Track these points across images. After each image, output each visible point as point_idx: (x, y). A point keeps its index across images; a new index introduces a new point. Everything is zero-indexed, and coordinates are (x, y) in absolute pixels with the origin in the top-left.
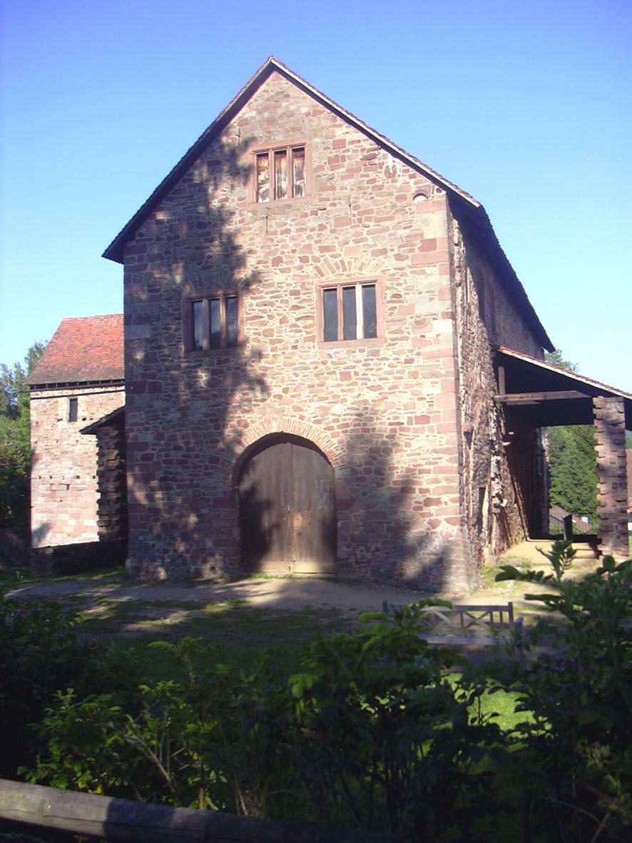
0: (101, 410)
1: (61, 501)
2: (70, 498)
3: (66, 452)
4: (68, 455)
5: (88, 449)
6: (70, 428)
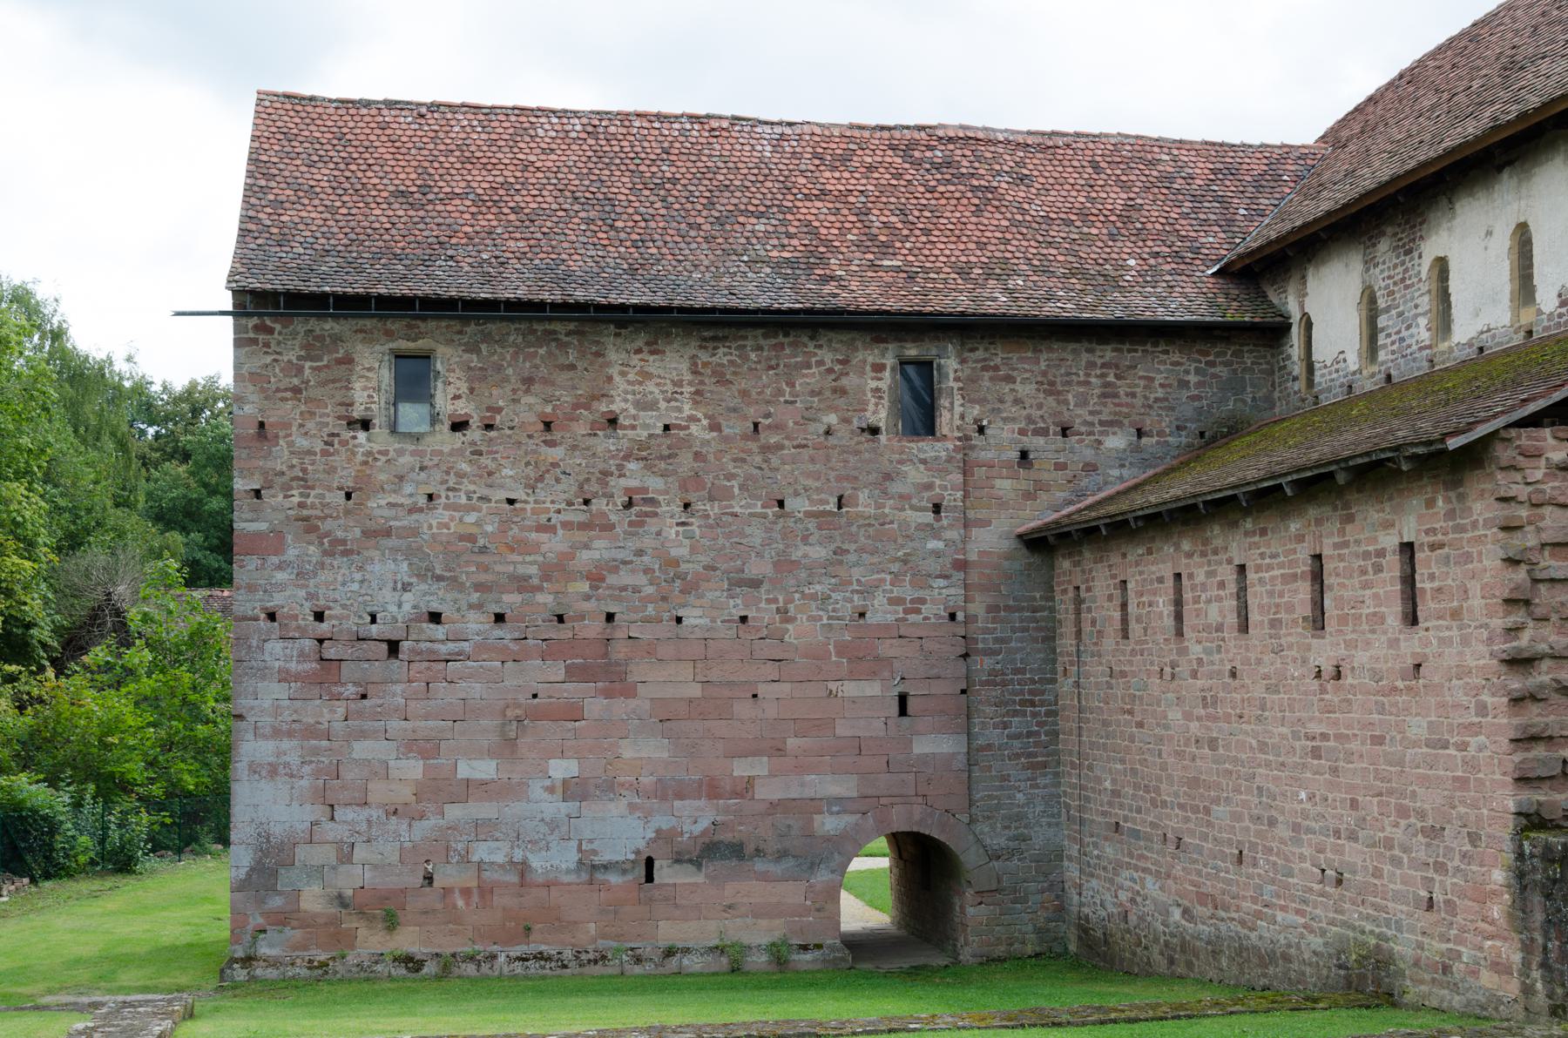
0: (530, 399)
1: (364, 697)
2: (398, 688)
3: (388, 533)
4: (392, 542)
5: (478, 524)
6: (400, 453)
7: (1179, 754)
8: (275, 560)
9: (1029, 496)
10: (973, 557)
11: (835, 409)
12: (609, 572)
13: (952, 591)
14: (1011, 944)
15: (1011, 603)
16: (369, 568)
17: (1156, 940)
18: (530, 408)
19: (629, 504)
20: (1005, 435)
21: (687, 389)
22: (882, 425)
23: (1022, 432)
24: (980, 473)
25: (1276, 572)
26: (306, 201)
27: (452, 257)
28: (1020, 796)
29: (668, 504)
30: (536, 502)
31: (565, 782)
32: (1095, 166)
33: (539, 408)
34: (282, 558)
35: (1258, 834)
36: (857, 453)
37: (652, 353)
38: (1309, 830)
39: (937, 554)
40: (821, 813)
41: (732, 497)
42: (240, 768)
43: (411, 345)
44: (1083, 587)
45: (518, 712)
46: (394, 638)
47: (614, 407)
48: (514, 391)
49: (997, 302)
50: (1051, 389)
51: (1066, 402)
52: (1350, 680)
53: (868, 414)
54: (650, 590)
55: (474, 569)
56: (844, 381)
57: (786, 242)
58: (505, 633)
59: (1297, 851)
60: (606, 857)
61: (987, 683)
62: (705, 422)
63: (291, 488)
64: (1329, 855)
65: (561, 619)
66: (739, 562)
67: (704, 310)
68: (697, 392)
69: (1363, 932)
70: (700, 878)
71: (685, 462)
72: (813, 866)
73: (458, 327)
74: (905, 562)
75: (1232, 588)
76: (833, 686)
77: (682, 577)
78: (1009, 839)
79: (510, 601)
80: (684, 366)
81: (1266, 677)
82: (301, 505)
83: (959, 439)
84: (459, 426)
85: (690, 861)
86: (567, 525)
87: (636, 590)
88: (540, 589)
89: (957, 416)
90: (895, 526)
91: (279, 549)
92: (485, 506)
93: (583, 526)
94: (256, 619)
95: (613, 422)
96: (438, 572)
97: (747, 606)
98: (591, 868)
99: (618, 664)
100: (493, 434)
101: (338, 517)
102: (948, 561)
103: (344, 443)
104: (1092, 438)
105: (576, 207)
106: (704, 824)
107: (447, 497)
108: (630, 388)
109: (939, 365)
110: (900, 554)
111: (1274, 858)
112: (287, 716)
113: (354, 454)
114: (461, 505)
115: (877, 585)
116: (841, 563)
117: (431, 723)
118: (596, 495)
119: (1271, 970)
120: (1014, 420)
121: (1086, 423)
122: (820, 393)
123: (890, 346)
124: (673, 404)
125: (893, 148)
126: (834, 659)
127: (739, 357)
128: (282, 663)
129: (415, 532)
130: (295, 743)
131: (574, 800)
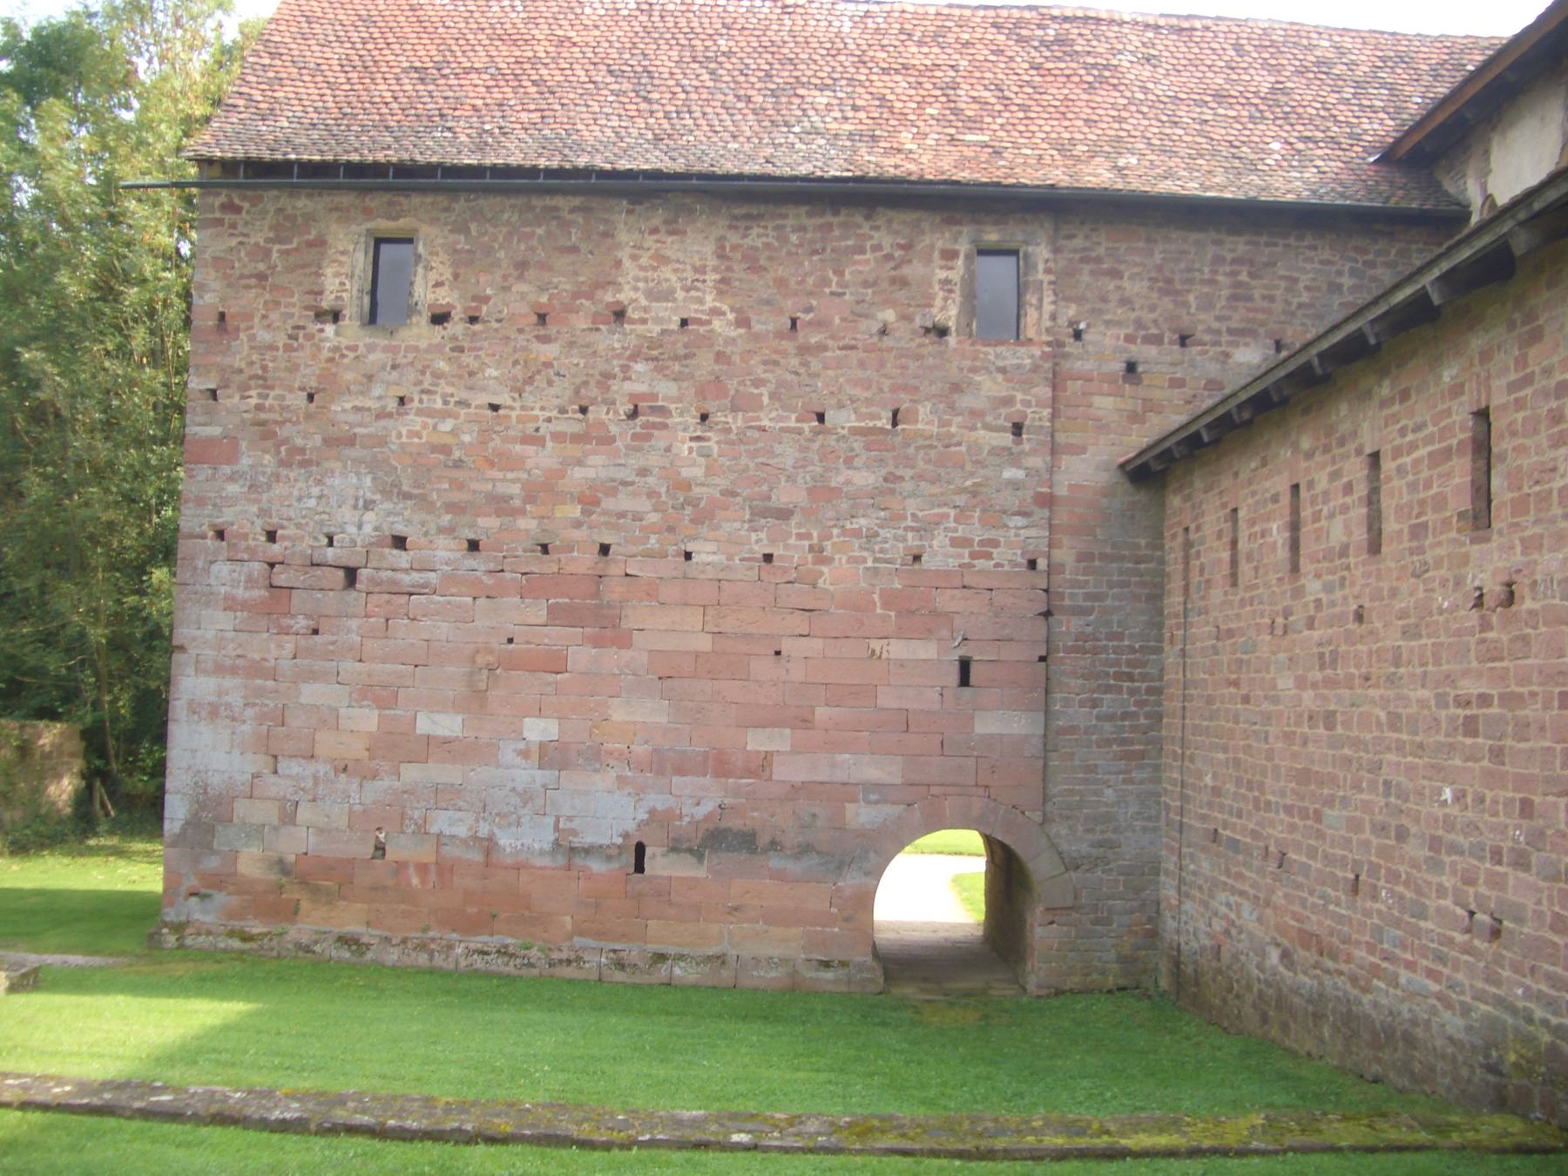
0: (523, 287)
1: (316, 632)
2: (354, 623)
3: (351, 441)
4: (356, 452)
5: (454, 432)
6: (371, 348)
7: (1289, 737)
8: (227, 469)
9: (1135, 418)
10: (1061, 491)
11: (889, 303)
12: (606, 495)
13: (1033, 532)
14: (1087, 975)
15: (1108, 550)
16: (328, 481)
17: (1249, 988)
18: (522, 297)
19: (634, 414)
20: (1107, 341)
21: (712, 277)
22: (951, 324)
23: (1129, 339)
24: (1074, 387)
25: (1422, 452)
26: (307, 78)
27: (449, 129)
28: (1109, 792)
29: (681, 415)
30: (523, 408)
31: (542, 746)
32: (1238, 48)
33: (532, 297)
34: (236, 468)
35: (1383, 851)
36: (919, 357)
37: (671, 233)
38: (1454, 849)
39: (1015, 485)
40: (854, 800)
41: (761, 407)
42: (179, 709)
43: (390, 224)
44: (1192, 527)
45: (490, 658)
46: (351, 564)
47: (621, 297)
48: (505, 277)
49: (1098, 176)
50: (1168, 288)
51: (1186, 305)
52: (1528, 604)
53: (935, 310)
54: (654, 518)
55: (446, 486)
56: (906, 271)
57: (850, 114)
58: (477, 563)
59: (1434, 879)
60: (589, 839)
61: (1075, 649)
62: (731, 316)
63: (249, 388)
64: (1482, 889)
65: (545, 549)
66: (765, 488)
67: (727, 177)
68: (723, 281)
69: (1530, 1020)
70: (701, 872)
71: (705, 364)
72: (840, 866)
73: (446, 204)
74: (974, 494)
75: (1361, 490)
76: (876, 645)
77: (694, 503)
78: (1092, 846)
79: (487, 524)
80: (709, 249)
81: (1403, 615)
82: (259, 408)
83: (1049, 344)
84: (440, 319)
85: (690, 850)
86: (558, 437)
87: (637, 517)
88: (522, 512)
89: (1046, 316)
90: (963, 449)
91: (232, 458)
92: (463, 412)
93: (577, 438)
94: (204, 537)
95: (620, 315)
96: (405, 488)
97: (772, 541)
98: (569, 851)
99: (609, 606)
100: (477, 327)
101: (297, 422)
102: (1028, 495)
103: (309, 337)
104: (1219, 349)
105: (609, 79)
106: (708, 807)
107: (421, 401)
108: (642, 274)
109: (1026, 254)
110: (968, 483)
111: (1400, 889)
112: (231, 650)
113: (319, 349)
114: (435, 411)
115: (938, 521)
116: (892, 492)
117: (388, 667)
118: (594, 401)
119: (1385, 1055)
120: (1119, 323)
121: (1210, 330)
122: (874, 284)
123: (965, 230)
124: (693, 293)
125: (994, 25)
126: (879, 611)
127: (777, 239)
128: (228, 589)
129: (382, 441)
130: (238, 681)
131: (551, 767)
